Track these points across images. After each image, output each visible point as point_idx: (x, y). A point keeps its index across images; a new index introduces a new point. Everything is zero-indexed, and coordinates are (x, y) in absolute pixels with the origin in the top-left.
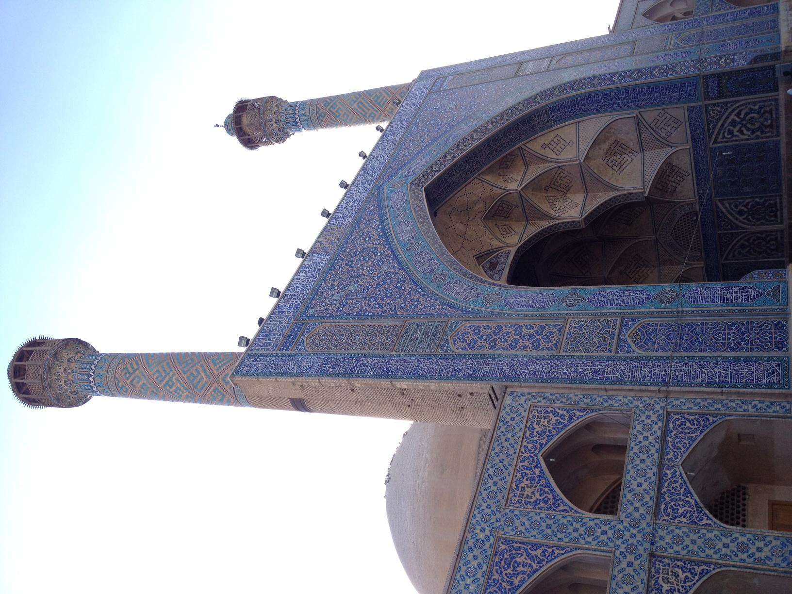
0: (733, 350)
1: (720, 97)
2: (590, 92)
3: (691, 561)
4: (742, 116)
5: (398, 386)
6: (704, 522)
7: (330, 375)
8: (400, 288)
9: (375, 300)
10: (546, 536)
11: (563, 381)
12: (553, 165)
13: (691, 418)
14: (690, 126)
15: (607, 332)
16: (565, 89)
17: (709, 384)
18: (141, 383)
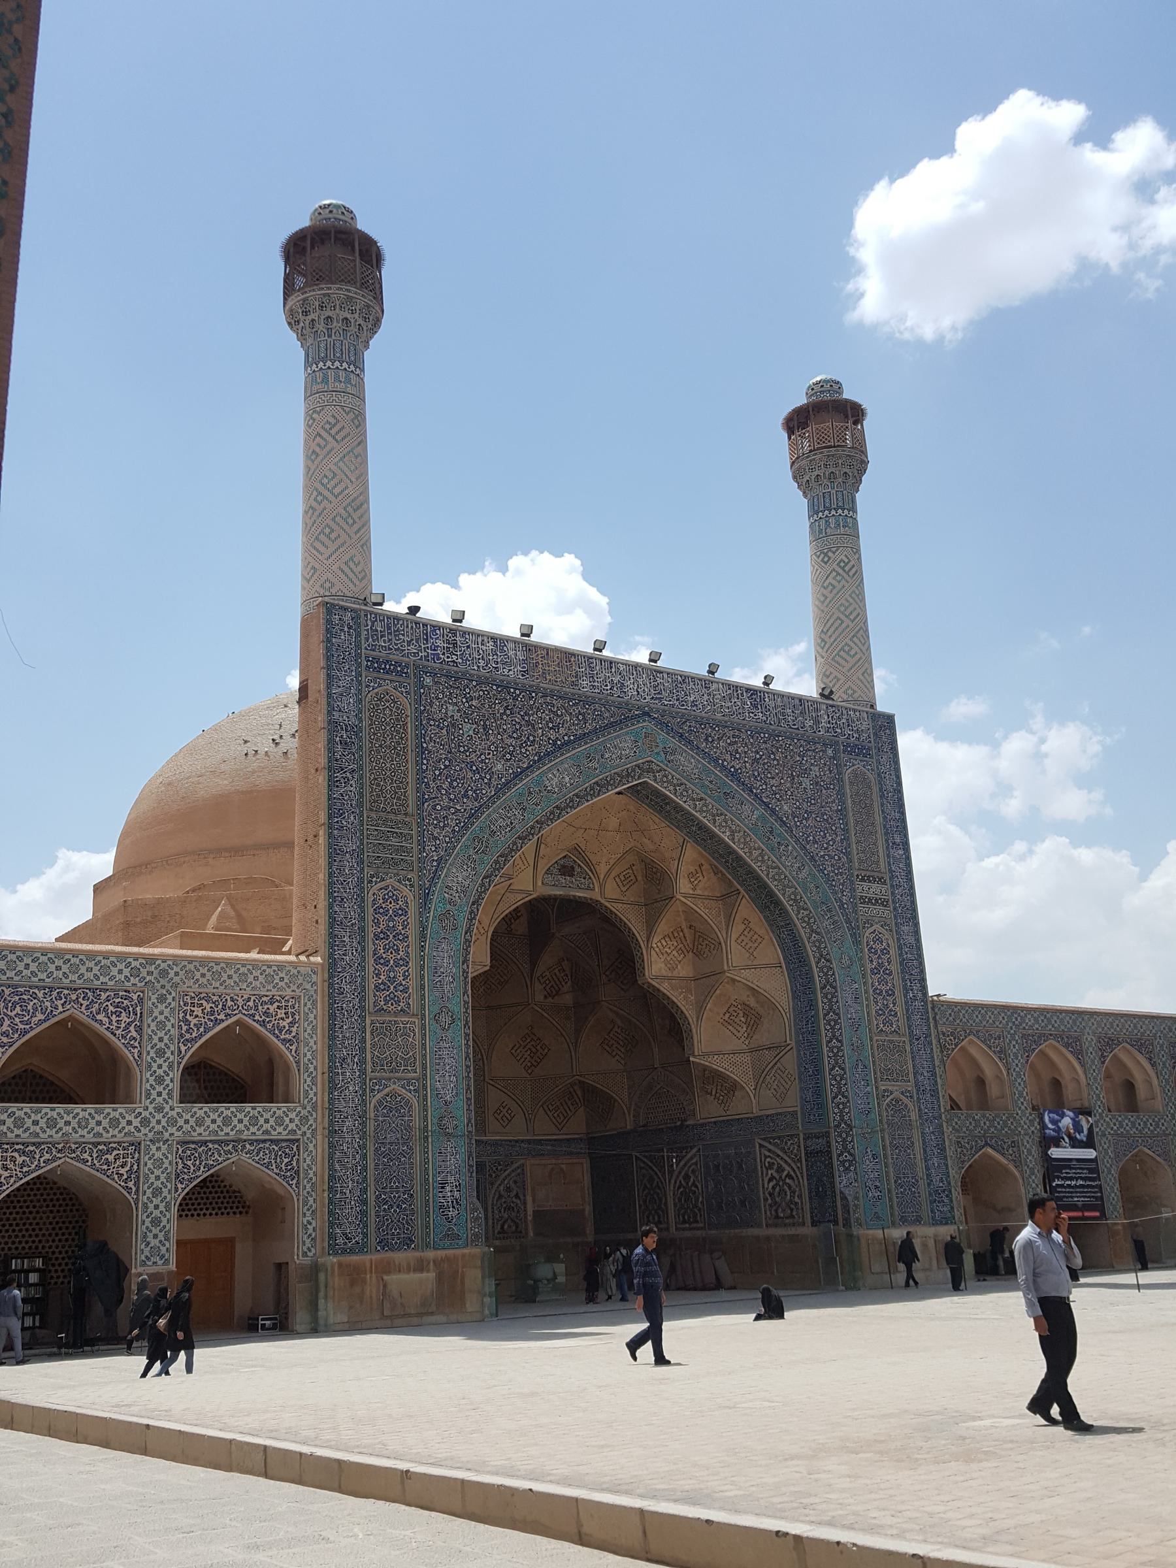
0: (377, 1197)
1: (806, 1154)
2: (814, 983)
3: (138, 1177)
4: (788, 1181)
5: (321, 833)
6: (179, 1186)
7: (331, 741)
8: (466, 795)
9: (446, 767)
10: (150, 1038)
11: (332, 1027)
12: (721, 936)
13: (294, 1164)
14: (777, 1114)
15: (399, 1064)
16: (819, 948)
17: (331, 1178)
18: (318, 450)
